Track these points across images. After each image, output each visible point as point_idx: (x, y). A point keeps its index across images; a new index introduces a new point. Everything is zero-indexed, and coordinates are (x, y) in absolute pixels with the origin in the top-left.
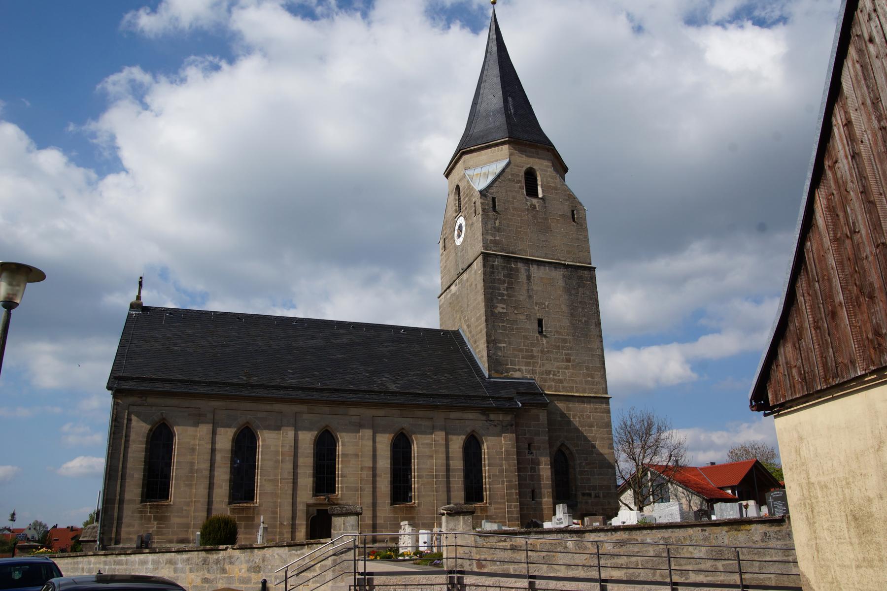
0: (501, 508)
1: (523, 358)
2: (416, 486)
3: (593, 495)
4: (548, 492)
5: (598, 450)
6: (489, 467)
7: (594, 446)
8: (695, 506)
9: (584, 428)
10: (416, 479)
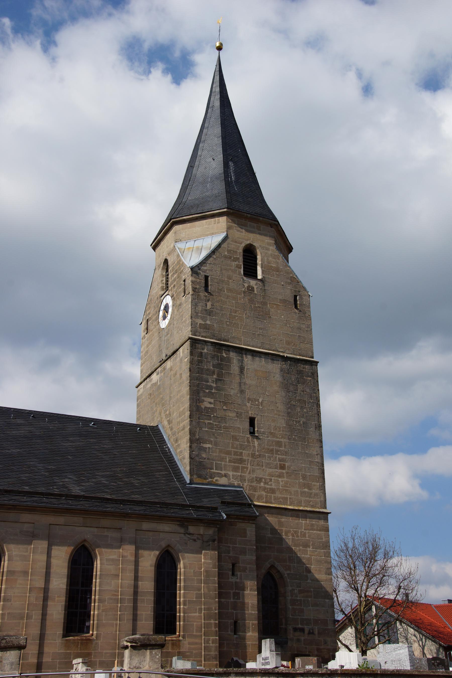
0: (196, 643)
1: (230, 461)
2: (96, 613)
3: (306, 631)
4: (253, 624)
5: (313, 575)
6: (184, 590)
7: (308, 571)
8: (430, 654)
9: (298, 548)
10: (96, 604)
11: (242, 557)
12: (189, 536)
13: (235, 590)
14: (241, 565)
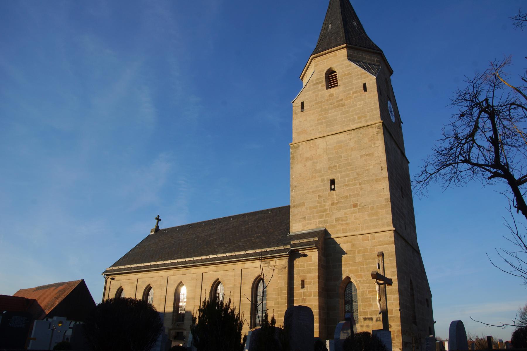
1: (317, 213)
3: (374, 319)
11: (308, 275)
12: (271, 267)
13: (303, 297)
14: (308, 280)
